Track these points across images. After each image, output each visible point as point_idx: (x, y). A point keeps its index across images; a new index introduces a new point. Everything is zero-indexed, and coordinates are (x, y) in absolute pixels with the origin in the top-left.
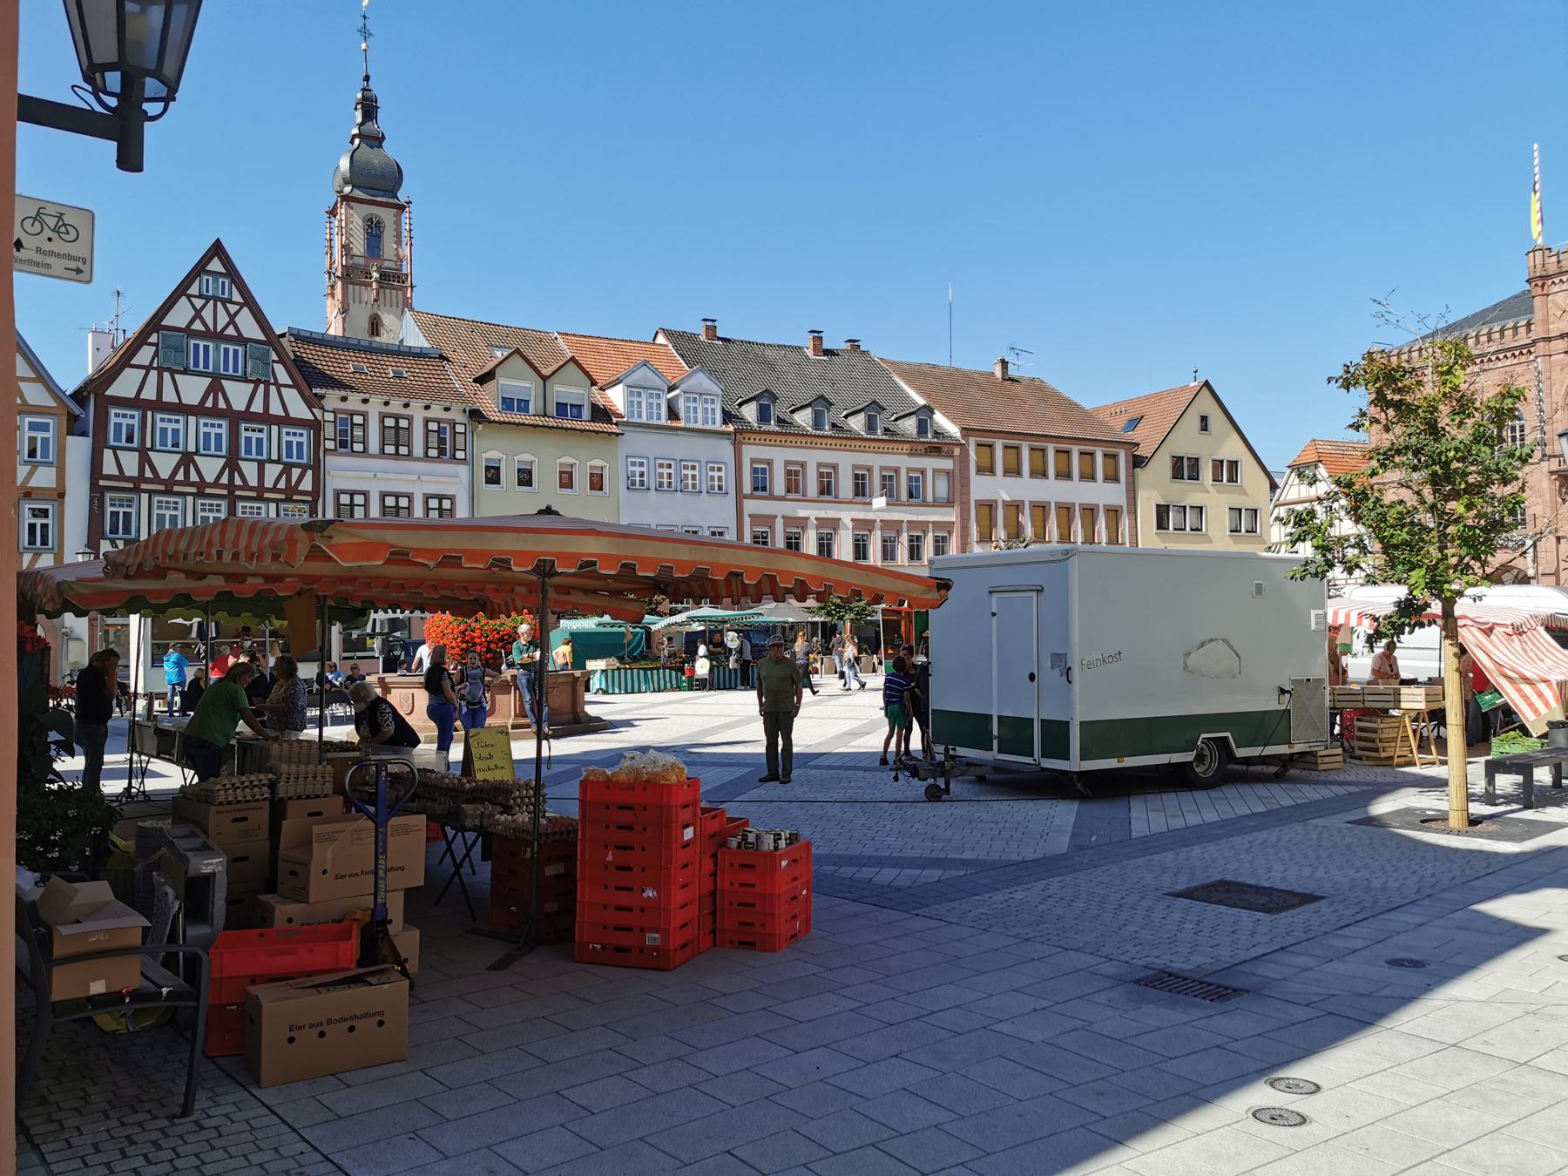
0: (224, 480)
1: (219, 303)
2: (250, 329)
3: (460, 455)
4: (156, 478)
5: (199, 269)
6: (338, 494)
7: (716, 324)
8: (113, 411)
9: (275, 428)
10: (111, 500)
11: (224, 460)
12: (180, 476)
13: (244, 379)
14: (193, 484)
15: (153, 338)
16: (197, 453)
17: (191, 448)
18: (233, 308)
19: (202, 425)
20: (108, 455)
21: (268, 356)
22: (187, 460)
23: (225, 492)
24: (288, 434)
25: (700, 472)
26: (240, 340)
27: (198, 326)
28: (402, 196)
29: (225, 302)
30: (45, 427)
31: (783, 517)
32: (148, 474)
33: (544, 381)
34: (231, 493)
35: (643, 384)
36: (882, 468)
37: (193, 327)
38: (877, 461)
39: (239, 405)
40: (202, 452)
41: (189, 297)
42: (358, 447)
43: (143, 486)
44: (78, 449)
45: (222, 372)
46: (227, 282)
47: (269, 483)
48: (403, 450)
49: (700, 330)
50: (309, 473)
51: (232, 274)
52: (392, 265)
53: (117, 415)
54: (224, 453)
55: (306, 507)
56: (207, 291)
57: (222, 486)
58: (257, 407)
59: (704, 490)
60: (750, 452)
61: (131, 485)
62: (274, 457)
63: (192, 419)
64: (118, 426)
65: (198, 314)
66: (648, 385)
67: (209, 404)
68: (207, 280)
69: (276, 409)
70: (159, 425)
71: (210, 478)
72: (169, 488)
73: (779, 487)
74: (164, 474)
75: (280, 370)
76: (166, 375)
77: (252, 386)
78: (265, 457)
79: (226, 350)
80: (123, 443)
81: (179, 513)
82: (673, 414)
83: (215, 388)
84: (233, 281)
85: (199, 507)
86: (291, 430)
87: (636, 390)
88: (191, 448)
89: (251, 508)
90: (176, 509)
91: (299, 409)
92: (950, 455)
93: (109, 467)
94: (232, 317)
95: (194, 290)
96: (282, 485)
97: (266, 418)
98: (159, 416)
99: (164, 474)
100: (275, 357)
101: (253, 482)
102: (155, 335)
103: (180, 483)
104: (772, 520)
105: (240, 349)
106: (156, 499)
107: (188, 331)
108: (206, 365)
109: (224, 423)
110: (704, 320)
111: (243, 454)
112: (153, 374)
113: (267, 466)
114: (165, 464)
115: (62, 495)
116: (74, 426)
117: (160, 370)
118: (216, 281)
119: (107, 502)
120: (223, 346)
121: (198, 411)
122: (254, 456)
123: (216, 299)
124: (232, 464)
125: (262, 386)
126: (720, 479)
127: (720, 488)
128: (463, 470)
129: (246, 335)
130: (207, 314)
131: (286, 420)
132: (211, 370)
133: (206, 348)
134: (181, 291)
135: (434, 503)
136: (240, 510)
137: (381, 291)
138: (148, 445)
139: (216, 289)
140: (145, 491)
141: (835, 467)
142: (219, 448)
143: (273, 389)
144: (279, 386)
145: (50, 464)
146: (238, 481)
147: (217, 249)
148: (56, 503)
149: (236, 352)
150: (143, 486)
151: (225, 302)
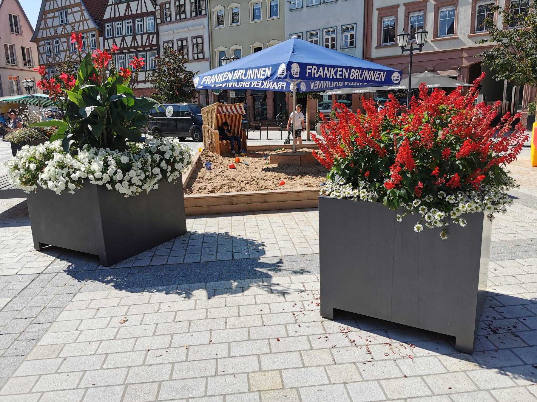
3: (203, 12)
6: (164, 42)
8: (106, 25)
17: (124, 34)
22: (123, 40)
31: (405, 5)
42: (169, 19)
48: (183, 16)
50: (155, 35)
55: (156, 52)
62: (145, 32)
76: (116, 6)
88: (124, 34)
96: (147, 44)
101: (140, 44)
113: (143, 36)
128: (205, 20)
135: (195, 41)
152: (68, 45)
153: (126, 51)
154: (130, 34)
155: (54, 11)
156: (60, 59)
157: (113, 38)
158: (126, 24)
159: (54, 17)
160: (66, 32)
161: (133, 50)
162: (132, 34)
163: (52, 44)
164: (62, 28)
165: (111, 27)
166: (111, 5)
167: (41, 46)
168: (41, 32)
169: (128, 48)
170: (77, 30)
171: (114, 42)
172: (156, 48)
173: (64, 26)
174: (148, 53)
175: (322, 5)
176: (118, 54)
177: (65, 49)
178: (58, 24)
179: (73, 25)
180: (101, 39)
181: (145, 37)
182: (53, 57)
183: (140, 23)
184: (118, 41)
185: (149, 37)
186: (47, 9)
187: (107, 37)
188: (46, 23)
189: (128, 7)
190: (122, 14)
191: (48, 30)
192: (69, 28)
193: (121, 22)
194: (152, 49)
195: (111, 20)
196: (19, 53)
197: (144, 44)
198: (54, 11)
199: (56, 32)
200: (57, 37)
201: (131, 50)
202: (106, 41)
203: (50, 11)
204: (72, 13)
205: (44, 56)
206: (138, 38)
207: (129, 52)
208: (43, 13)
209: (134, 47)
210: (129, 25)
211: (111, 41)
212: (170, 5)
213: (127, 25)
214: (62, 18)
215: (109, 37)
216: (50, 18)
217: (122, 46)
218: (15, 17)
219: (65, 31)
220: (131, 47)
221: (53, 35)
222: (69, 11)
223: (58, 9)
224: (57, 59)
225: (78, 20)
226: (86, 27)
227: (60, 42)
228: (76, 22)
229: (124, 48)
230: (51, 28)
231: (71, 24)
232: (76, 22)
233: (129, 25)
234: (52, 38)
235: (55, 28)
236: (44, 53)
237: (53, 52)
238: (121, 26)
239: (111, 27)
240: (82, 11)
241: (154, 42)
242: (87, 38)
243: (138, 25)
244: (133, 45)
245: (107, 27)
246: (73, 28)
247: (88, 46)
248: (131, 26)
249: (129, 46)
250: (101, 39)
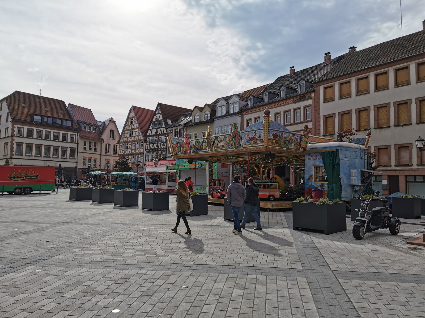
13: (159, 128)
18: (160, 114)
22: (153, 145)
35: (221, 105)
60: (246, 117)
88: (154, 143)
92: (310, 98)
96: (162, 147)
101: (159, 148)
115: (144, 153)
122: (152, 143)
152: (131, 146)
153: (153, 150)
154: (156, 143)
155: (128, 130)
156: (128, 152)
157: (149, 144)
158: (155, 138)
159: (128, 133)
160: (132, 140)
161: (157, 150)
162: (157, 143)
163: (125, 145)
164: (130, 138)
165: (149, 139)
166: (150, 129)
167: (121, 145)
168: (122, 139)
169: (155, 149)
170: (136, 139)
171: (150, 146)
172: (165, 149)
173: (131, 137)
174: (162, 151)
176: (151, 151)
177: (130, 147)
178: (129, 136)
179: (135, 137)
180: (145, 144)
181: (162, 144)
182: (125, 151)
184: (151, 145)
185: (163, 144)
186: (125, 129)
187: (147, 143)
188: (124, 135)
189: (157, 131)
190: (154, 134)
191: (124, 138)
192: (133, 138)
193: (153, 137)
194: (164, 150)
195: (150, 136)
196: (112, 148)
197: (161, 148)
198: (128, 130)
199: (127, 140)
200: (127, 142)
201: (156, 150)
202: (147, 145)
203: (127, 130)
204: (135, 132)
205: (121, 150)
206: (159, 144)
207: (155, 151)
208: (124, 130)
209: (157, 149)
210: (156, 138)
211: (148, 145)
212: (172, 131)
213: (155, 139)
214: (131, 133)
215: (148, 143)
216: (126, 133)
217: (152, 148)
218: (113, 131)
220: (156, 149)
221: (126, 141)
222: (134, 131)
223: (130, 130)
224: (126, 152)
225: (137, 135)
226: (140, 139)
227: (128, 144)
228: (136, 136)
229: (154, 149)
230: (126, 138)
231: (134, 136)
232: (136, 136)
233: (156, 138)
234: (125, 142)
235: (127, 138)
236: (121, 149)
237: (125, 149)
238: (153, 139)
239: (149, 139)
240: (139, 131)
241: (165, 147)
242: (140, 143)
243: (160, 139)
244: (157, 148)
245: (148, 139)
246: (134, 138)
247: (139, 147)
248: (157, 139)
249: (155, 148)
250: (145, 144)
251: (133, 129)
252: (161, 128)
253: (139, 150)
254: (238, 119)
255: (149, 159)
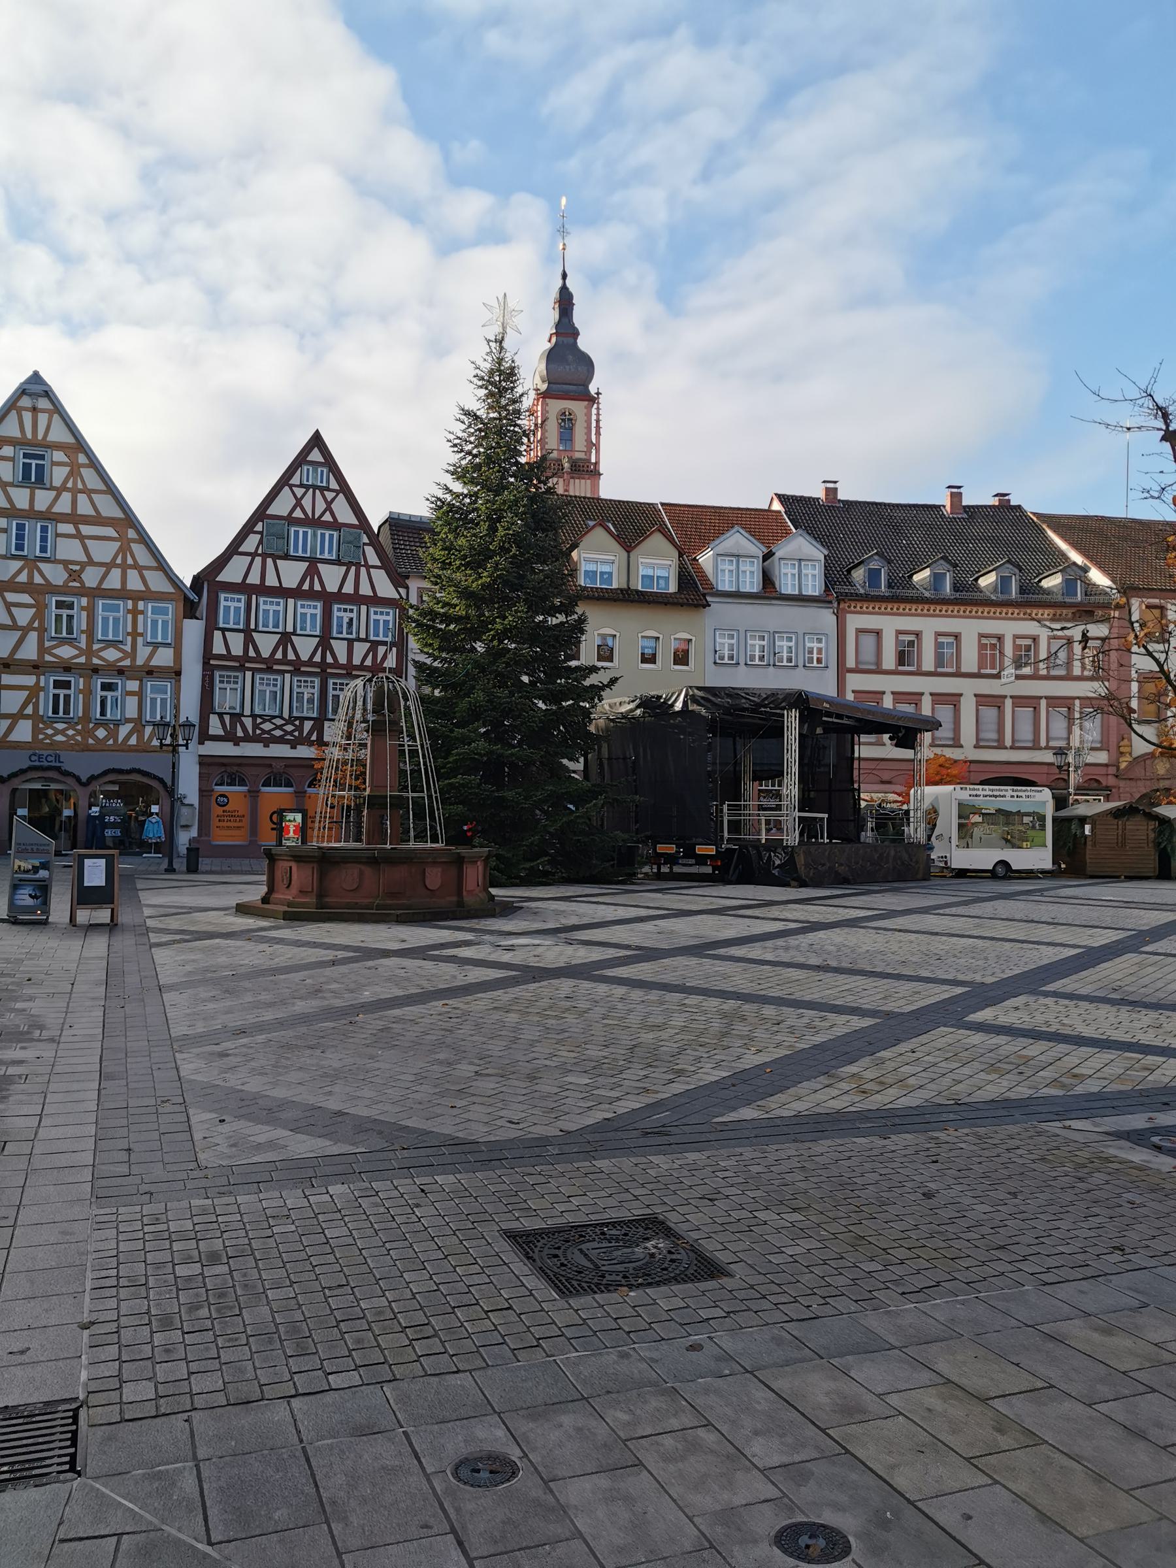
0: (317, 658)
1: (317, 491)
2: (345, 515)
4: (259, 658)
5: (301, 460)
7: (837, 485)
8: (222, 596)
9: (364, 608)
10: (220, 676)
11: (318, 639)
12: (279, 655)
13: (338, 562)
14: (290, 663)
15: (259, 527)
16: (294, 633)
17: (290, 629)
18: (330, 495)
19: (299, 606)
20: (217, 635)
21: (359, 537)
22: (286, 639)
23: (318, 670)
24: (376, 613)
25: (797, 643)
26: (335, 525)
27: (298, 514)
28: (592, 389)
29: (322, 489)
30: (165, 612)
31: (893, 693)
32: (252, 653)
33: (628, 552)
34: (323, 671)
35: (735, 552)
36: (1016, 637)
37: (293, 515)
38: (1012, 628)
39: (332, 587)
40: (299, 632)
41: (291, 487)
43: (247, 665)
44: (193, 630)
45: (318, 556)
46: (325, 470)
47: (356, 661)
49: (819, 493)
51: (330, 463)
52: (582, 456)
53: (226, 600)
54: (318, 633)
56: (308, 481)
57: (315, 665)
58: (349, 588)
59: (801, 664)
60: (855, 622)
61: (237, 664)
62: (362, 635)
63: (291, 602)
64: (340, 619)
65: (298, 503)
66: (741, 552)
67: (306, 587)
68: (308, 470)
69: (365, 590)
70: (262, 607)
71: (305, 657)
72: (268, 666)
73: (889, 661)
74: (265, 654)
75: (370, 552)
76: (269, 561)
77: (345, 568)
78: (354, 636)
79: (323, 535)
80: (231, 626)
81: (278, 689)
82: (768, 580)
83: (312, 571)
84: (330, 470)
85: (296, 683)
86: (343, 607)
87: (727, 558)
88: (290, 629)
89: (305, 681)
90: (275, 685)
91: (386, 588)
93: (218, 648)
94: (329, 504)
95: (295, 480)
96: (368, 662)
97: (356, 599)
98: (261, 600)
99: (265, 654)
100: (366, 540)
101: (343, 660)
102: (260, 524)
103: (279, 662)
104: (878, 696)
105: (335, 534)
106: (258, 677)
107: (290, 520)
108: (304, 550)
109: (319, 605)
110: (824, 482)
111: (335, 635)
112: (258, 560)
114: (266, 644)
115: (178, 673)
116: (190, 610)
117: (264, 556)
118: (315, 471)
119: (217, 679)
120: (319, 532)
121: (296, 593)
123: (315, 487)
124: (325, 642)
125: (353, 568)
126: (820, 651)
127: (819, 661)
129: (340, 520)
130: (307, 503)
131: (375, 600)
132: (308, 555)
133: (305, 534)
134: (284, 481)
136: (316, 685)
137: (572, 481)
138: (253, 626)
139: (315, 478)
140: (249, 669)
141: (957, 636)
142: (313, 626)
143: (363, 570)
144: (368, 567)
145: (167, 645)
146: (329, 660)
147: (317, 441)
148: (173, 681)
149: (331, 536)
150: (247, 665)
151: (322, 489)
175: (771, 667)
183: (346, 616)
219: (31, 576)
246: (75, 575)
251: (50, 517)
252: (349, 565)
253: (128, 648)
254: (826, 618)
255: (247, 712)
